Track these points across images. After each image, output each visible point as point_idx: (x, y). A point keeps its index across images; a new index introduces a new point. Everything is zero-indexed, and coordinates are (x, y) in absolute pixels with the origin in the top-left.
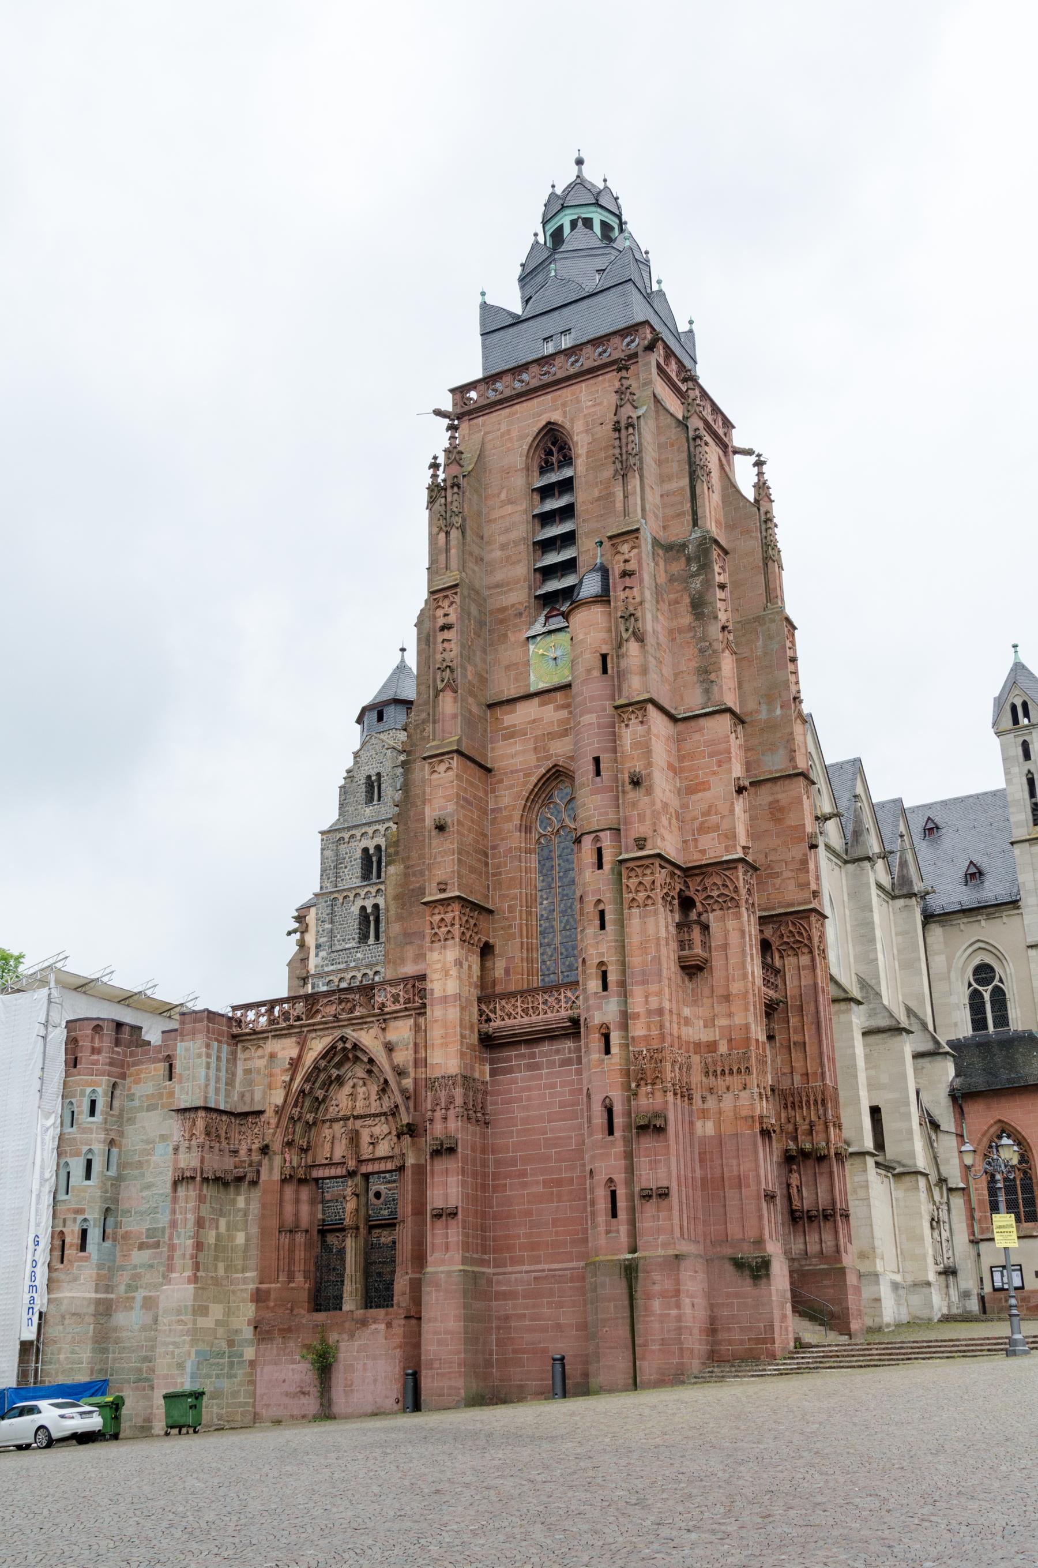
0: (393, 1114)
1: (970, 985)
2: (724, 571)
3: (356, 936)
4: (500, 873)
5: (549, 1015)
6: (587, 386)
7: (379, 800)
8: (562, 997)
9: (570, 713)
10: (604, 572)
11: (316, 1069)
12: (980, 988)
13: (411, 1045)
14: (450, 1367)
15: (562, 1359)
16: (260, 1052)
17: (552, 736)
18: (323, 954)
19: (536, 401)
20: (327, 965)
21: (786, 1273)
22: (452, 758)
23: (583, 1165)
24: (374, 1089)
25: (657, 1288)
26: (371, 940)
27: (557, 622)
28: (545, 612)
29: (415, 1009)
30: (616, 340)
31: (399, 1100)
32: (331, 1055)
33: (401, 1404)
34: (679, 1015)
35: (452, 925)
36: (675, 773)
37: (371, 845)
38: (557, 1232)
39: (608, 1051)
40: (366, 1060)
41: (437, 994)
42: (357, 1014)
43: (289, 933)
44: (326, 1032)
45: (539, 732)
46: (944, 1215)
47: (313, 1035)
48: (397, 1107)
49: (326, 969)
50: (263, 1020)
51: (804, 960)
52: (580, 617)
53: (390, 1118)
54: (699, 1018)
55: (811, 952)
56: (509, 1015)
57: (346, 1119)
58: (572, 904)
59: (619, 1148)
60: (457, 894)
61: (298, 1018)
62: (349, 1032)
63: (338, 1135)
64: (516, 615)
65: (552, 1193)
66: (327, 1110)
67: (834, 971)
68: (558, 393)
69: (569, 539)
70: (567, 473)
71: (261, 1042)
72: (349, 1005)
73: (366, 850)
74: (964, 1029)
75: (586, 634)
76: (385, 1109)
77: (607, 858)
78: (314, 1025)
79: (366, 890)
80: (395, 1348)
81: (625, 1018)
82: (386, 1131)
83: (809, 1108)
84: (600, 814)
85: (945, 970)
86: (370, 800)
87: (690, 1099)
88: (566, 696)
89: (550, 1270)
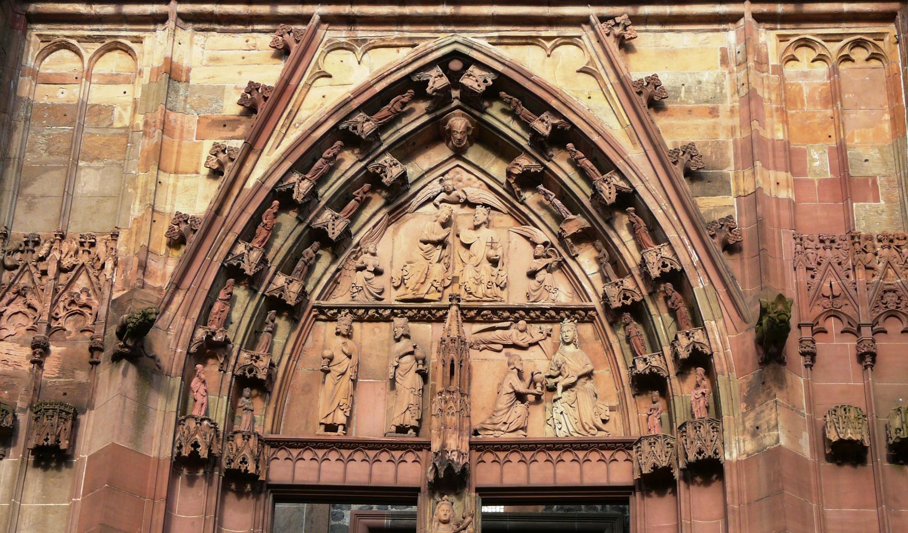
11: (342, 135)
16: (114, 62)
32: (394, 104)
44: (393, 34)
62: (478, 40)
66: (334, 281)
71: (125, 33)
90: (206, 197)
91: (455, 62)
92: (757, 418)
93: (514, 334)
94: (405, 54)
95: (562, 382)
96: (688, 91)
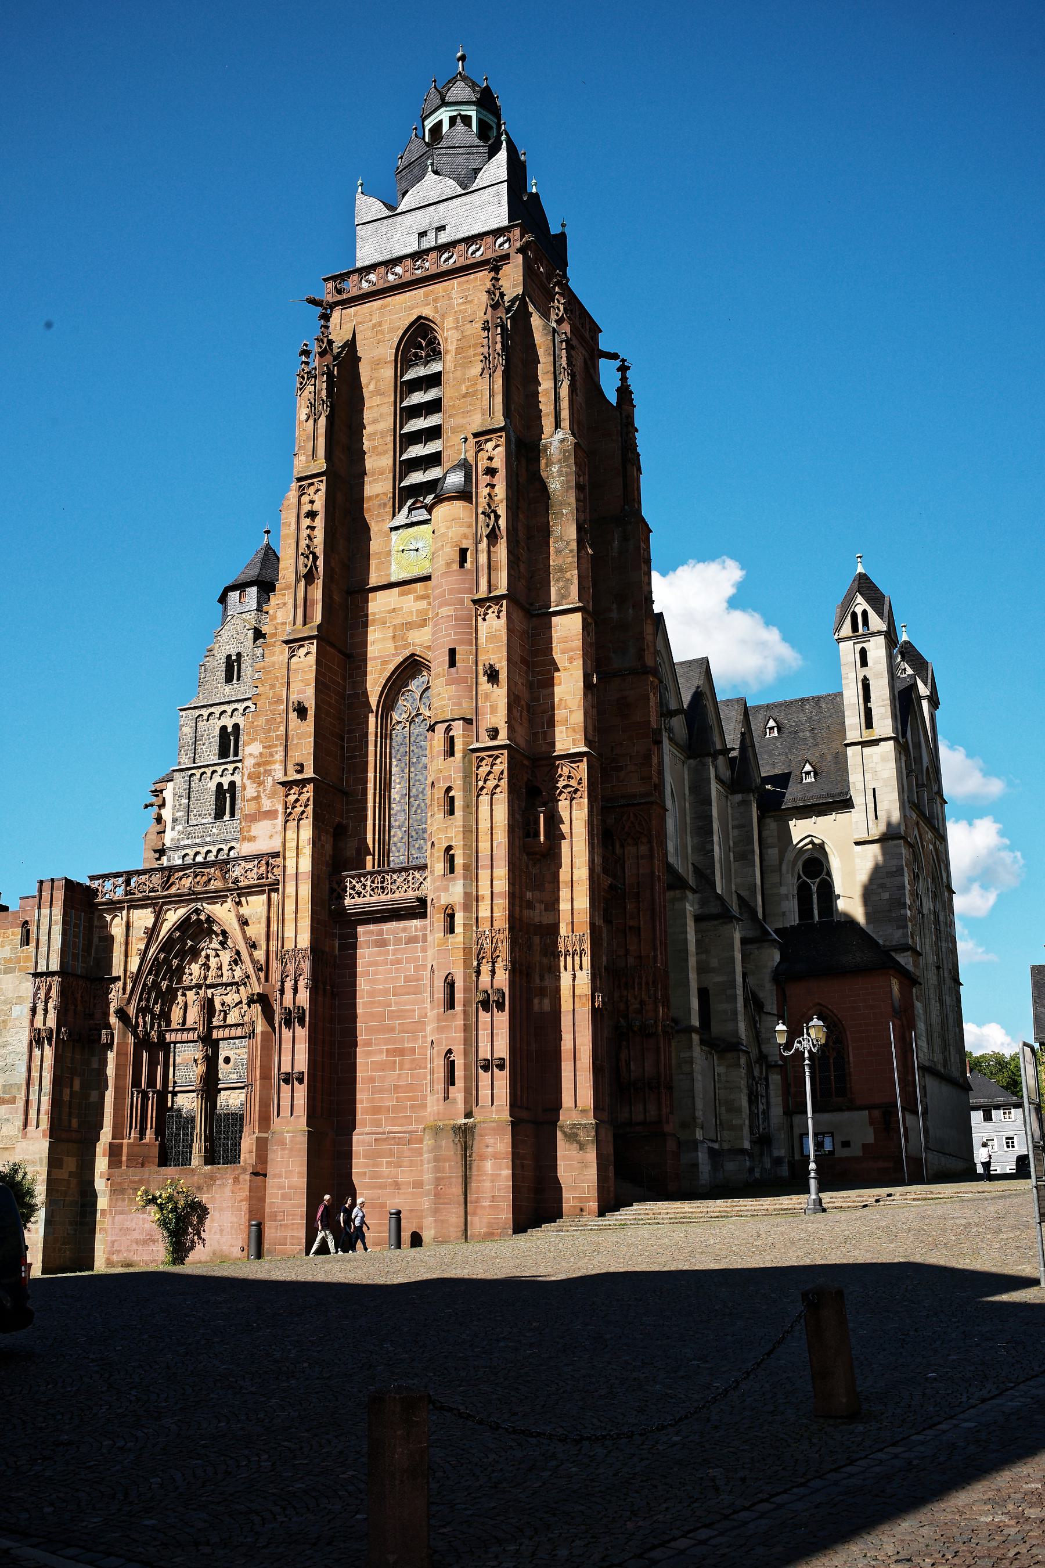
0: (245, 984)
1: (799, 877)
2: (584, 474)
3: (213, 812)
4: (355, 757)
5: (397, 895)
6: (459, 284)
7: (238, 679)
8: (410, 878)
9: (429, 604)
10: (466, 467)
12: (809, 881)
13: (264, 920)
14: (293, 1219)
15: (399, 1213)
17: (410, 626)
18: (179, 828)
19: (408, 294)
20: (183, 839)
21: (610, 1138)
22: (312, 644)
23: (425, 1037)
24: (226, 957)
25: (490, 1150)
26: (227, 817)
27: (421, 515)
28: (410, 502)
29: (268, 885)
30: (489, 239)
31: (251, 971)
33: (246, 1251)
34: (521, 899)
35: (306, 806)
36: (528, 667)
37: (229, 723)
39: (452, 930)
40: (219, 932)
41: (291, 870)
42: (211, 887)
43: (146, 806)
45: (398, 621)
46: (761, 1089)
48: (248, 977)
49: (182, 843)
50: (120, 893)
51: (643, 849)
52: (442, 511)
53: (242, 988)
54: (541, 902)
55: (650, 842)
56: (359, 894)
57: (199, 987)
58: (424, 789)
59: (460, 1022)
60: (313, 775)
61: (153, 890)
63: (190, 1003)
64: (380, 505)
65: (395, 1061)
67: (671, 860)
68: (430, 288)
69: (434, 433)
70: (436, 367)
72: (205, 878)
73: (224, 728)
74: (794, 919)
75: (448, 528)
76: (237, 979)
77: (459, 746)
78: (170, 896)
79: (223, 767)
80: (242, 1201)
81: (472, 900)
82: (237, 1001)
83: (640, 989)
84: (454, 704)
85: (777, 863)
86: (229, 679)
87: (528, 975)
88: (426, 588)
89: (390, 1133)
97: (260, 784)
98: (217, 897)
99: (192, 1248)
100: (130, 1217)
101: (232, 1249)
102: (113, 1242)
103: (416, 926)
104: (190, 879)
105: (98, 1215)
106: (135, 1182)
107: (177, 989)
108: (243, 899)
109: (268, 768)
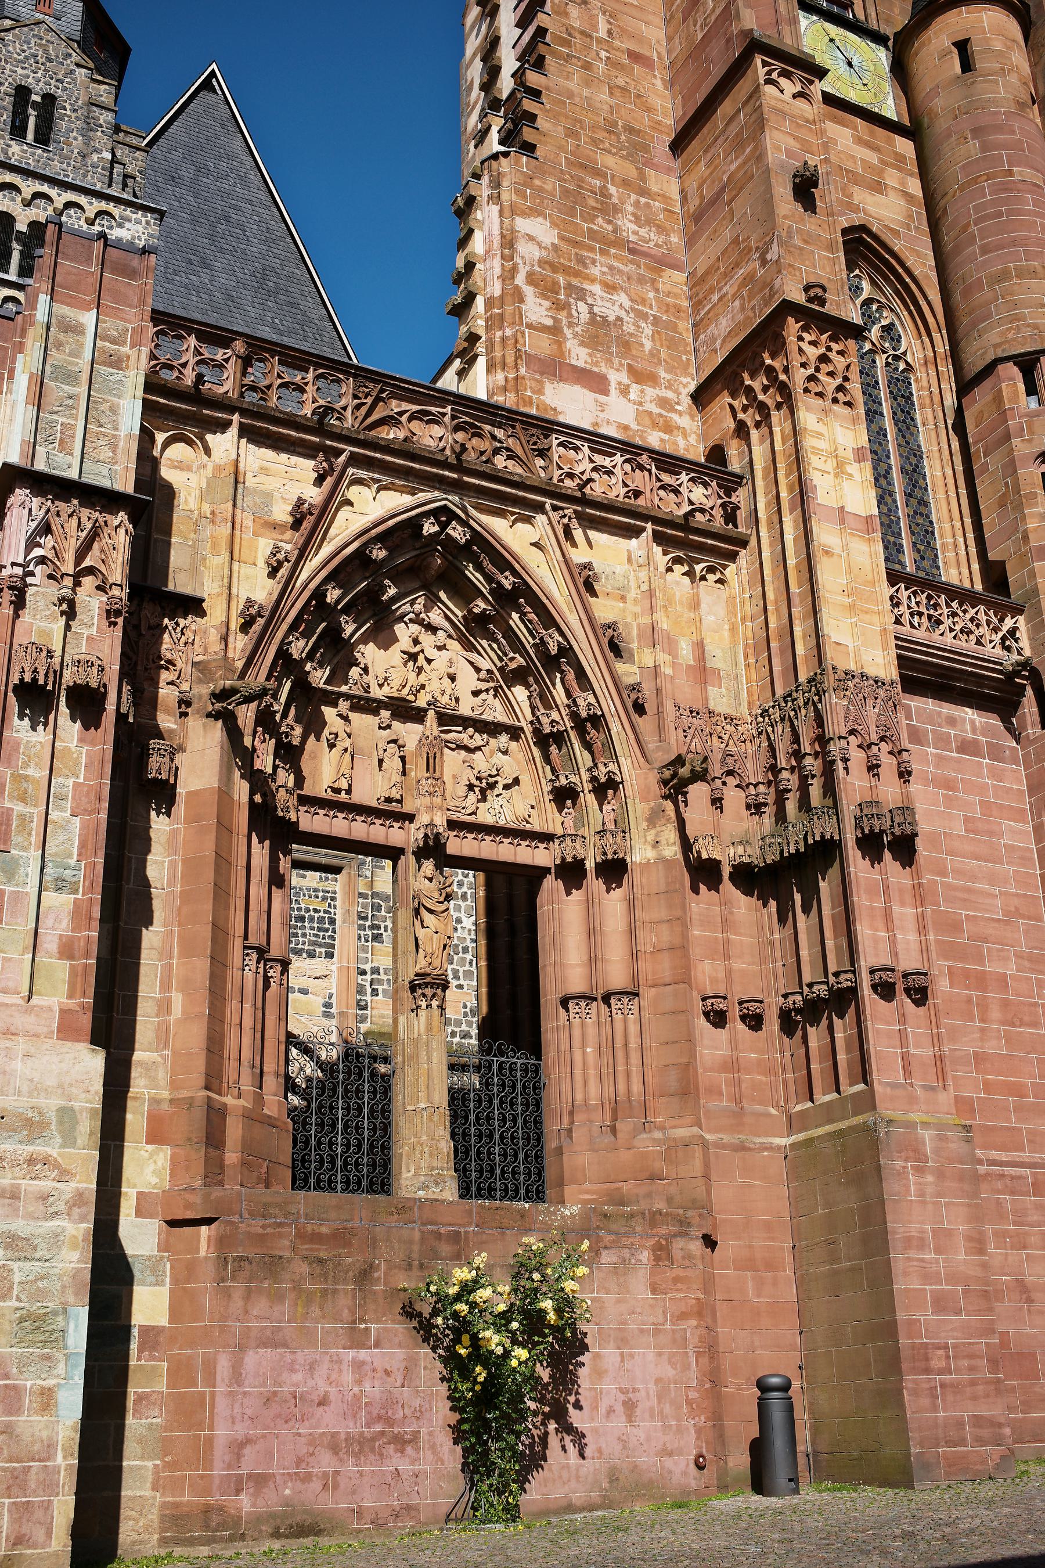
14: (972, 1369)
29: (656, 520)
38: (986, 1084)
47: (363, 474)
65: (969, 1001)
78: (386, 448)
80: (683, 1316)
90: (264, 587)
91: (444, 515)
92: (657, 835)
93: (464, 738)
94: (407, 500)
95: (502, 782)
96: (607, 578)
97: (559, 306)
98: (521, 499)
99: (534, 1460)
100: (303, 1355)
101: (668, 1463)
102: (238, 1447)
103: (972, 722)
104: (437, 431)
105: (134, 1346)
106: (316, 1238)
107: (332, 700)
108: (578, 534)
109: (575, 282)
